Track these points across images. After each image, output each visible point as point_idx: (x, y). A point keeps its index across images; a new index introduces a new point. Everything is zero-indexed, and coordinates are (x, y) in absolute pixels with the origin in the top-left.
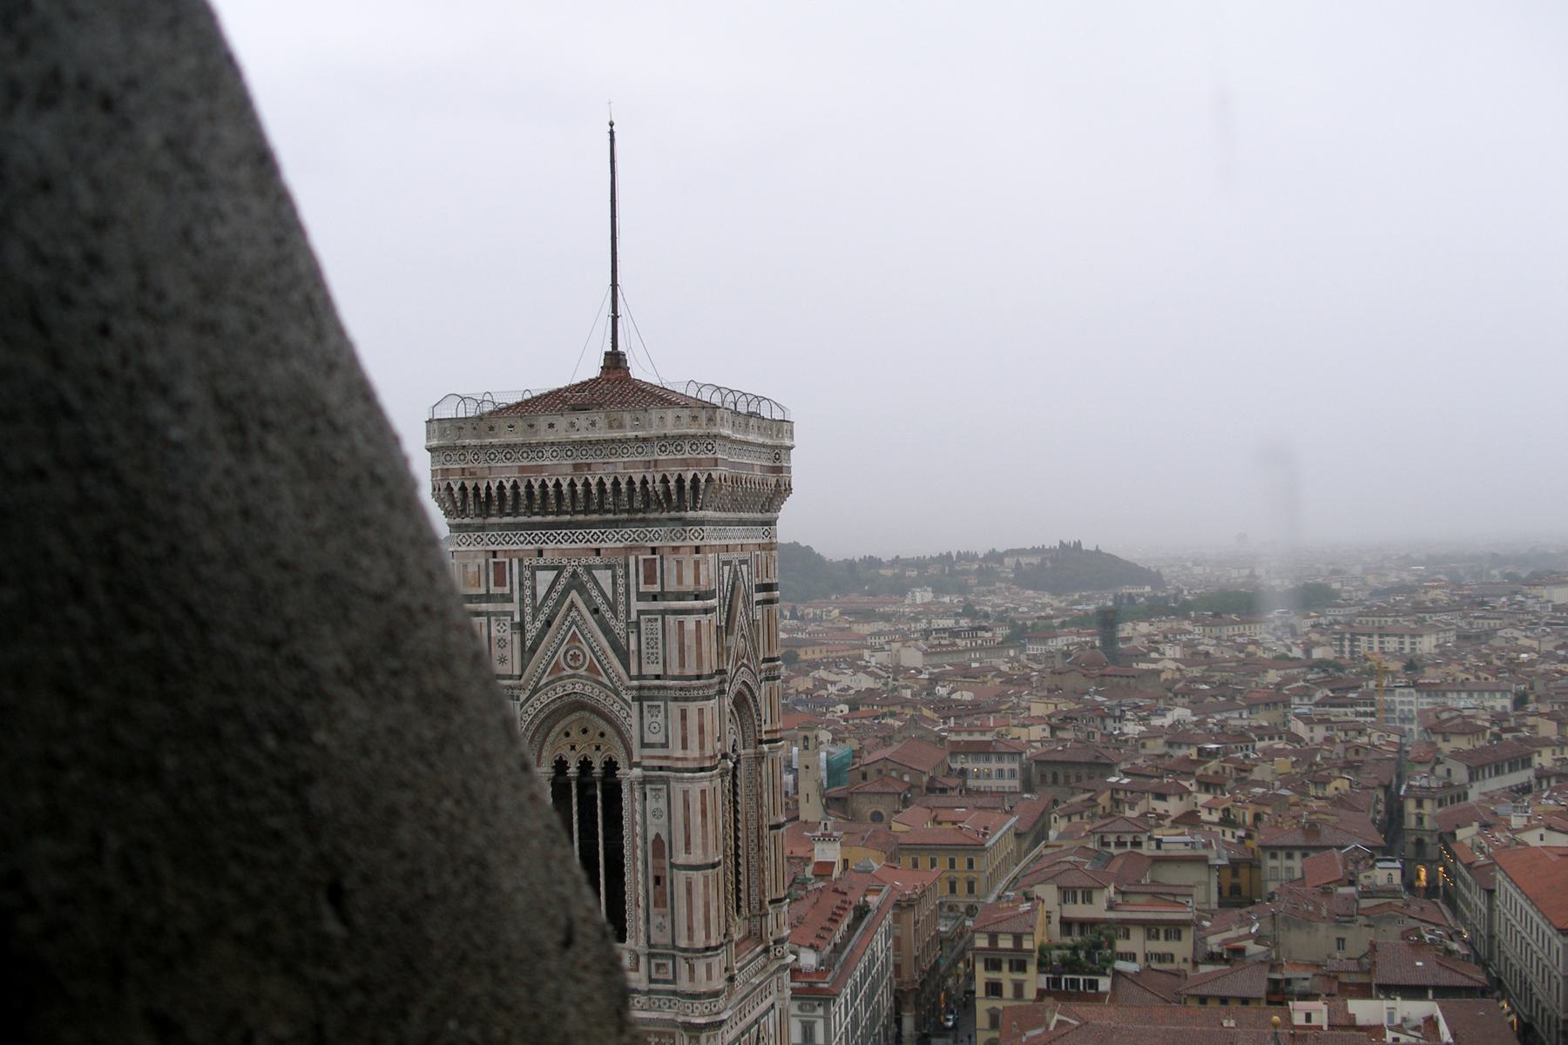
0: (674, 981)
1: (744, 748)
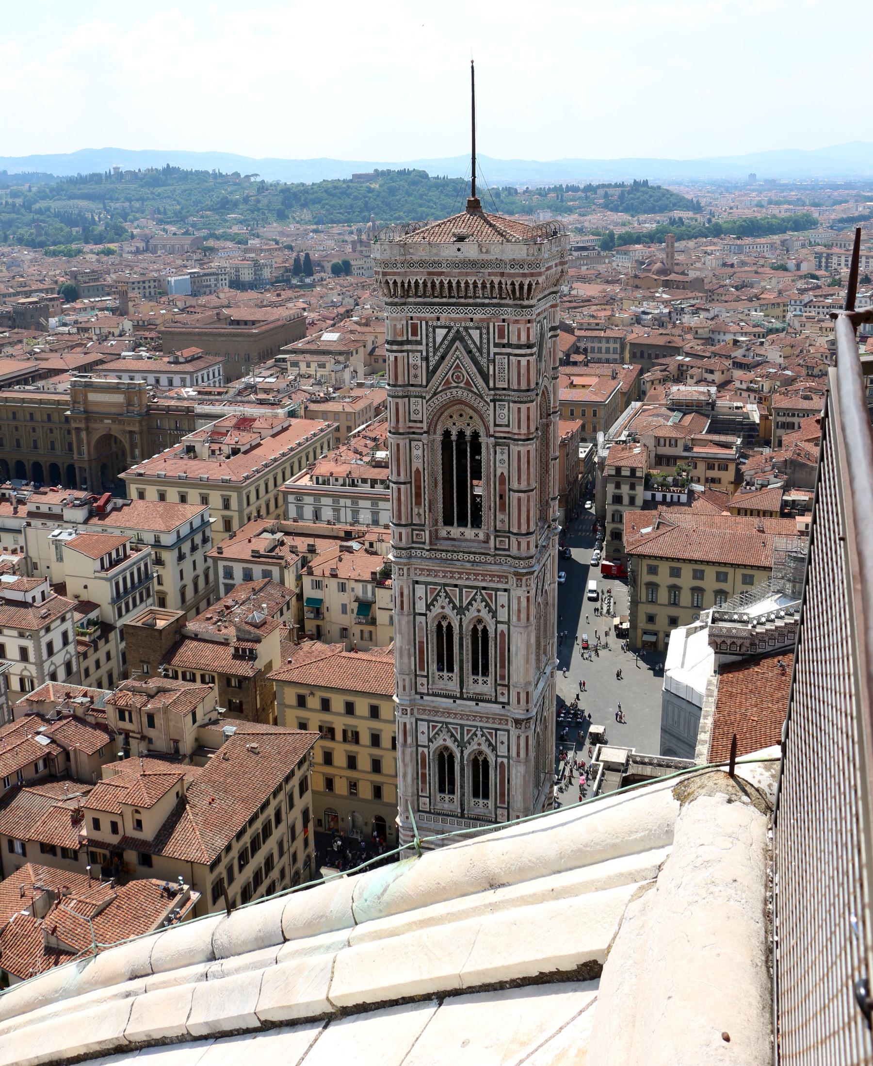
0: (508, 550)
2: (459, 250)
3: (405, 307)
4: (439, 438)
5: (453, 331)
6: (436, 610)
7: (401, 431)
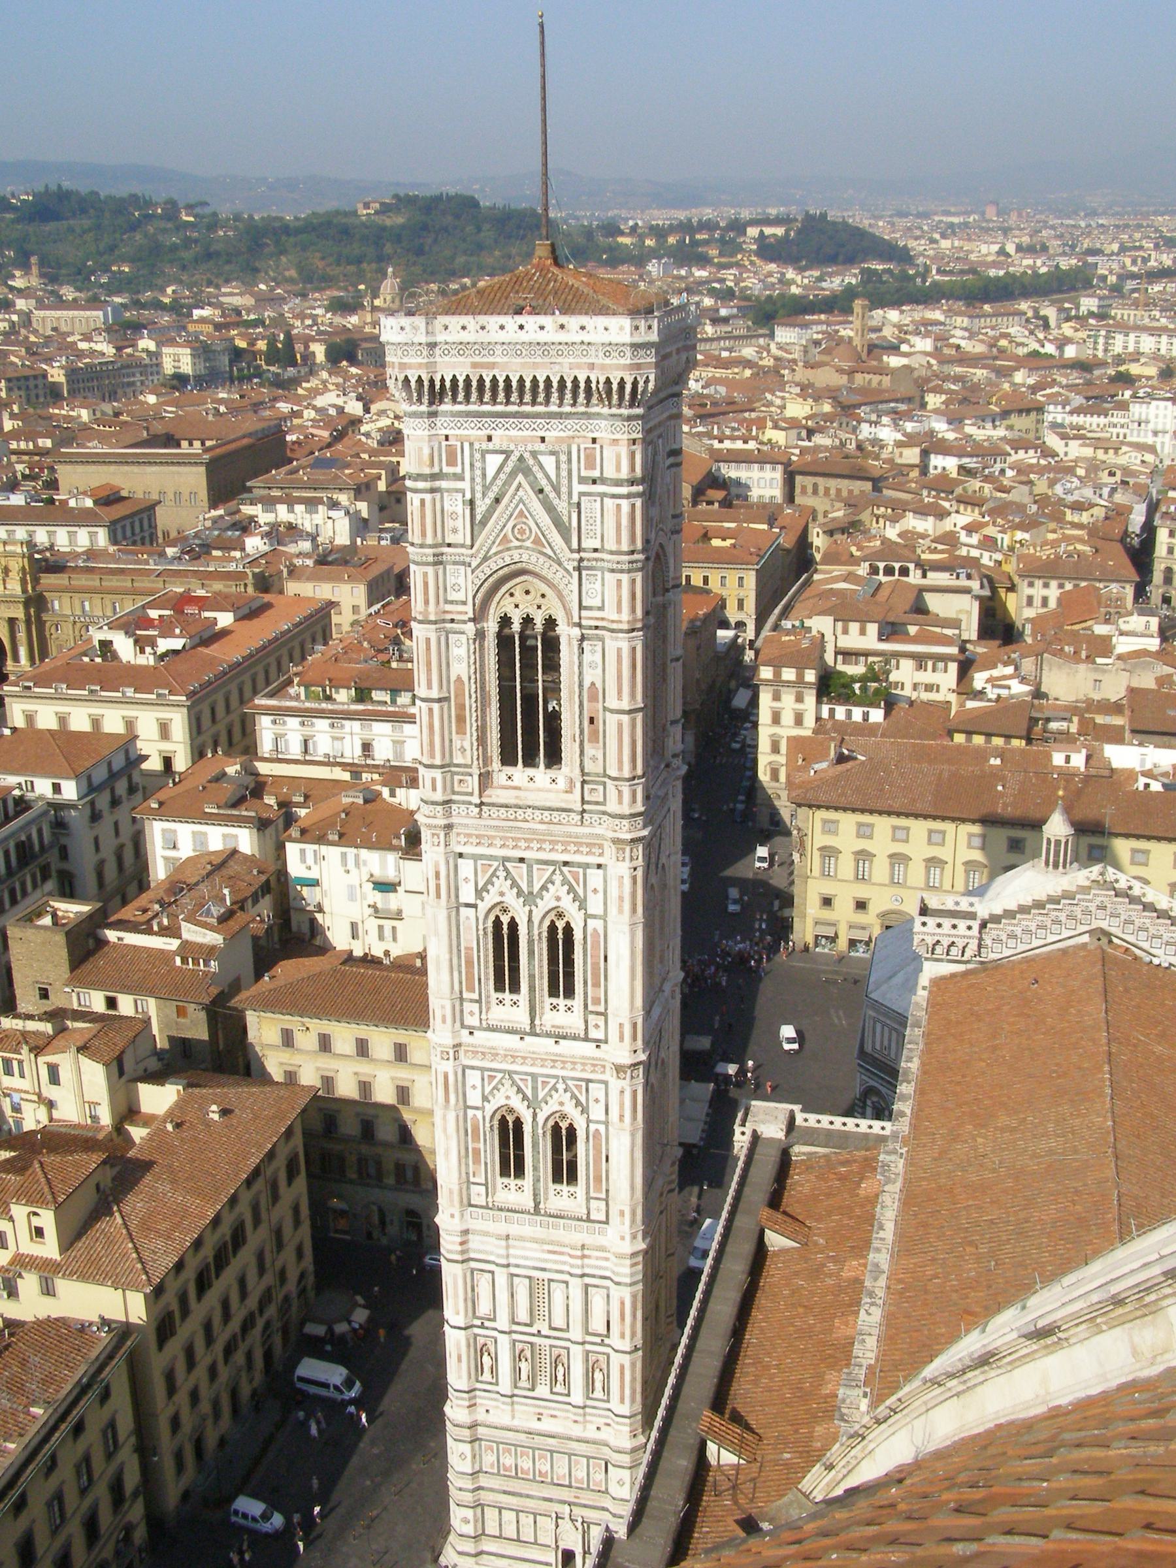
0: (604, 803)
1: (654, 595)
2: (521, 327)
3: (439, 421)
4: (491, 626)
5: (514, 458)
6: (491, 899)
7: (432, 618)
